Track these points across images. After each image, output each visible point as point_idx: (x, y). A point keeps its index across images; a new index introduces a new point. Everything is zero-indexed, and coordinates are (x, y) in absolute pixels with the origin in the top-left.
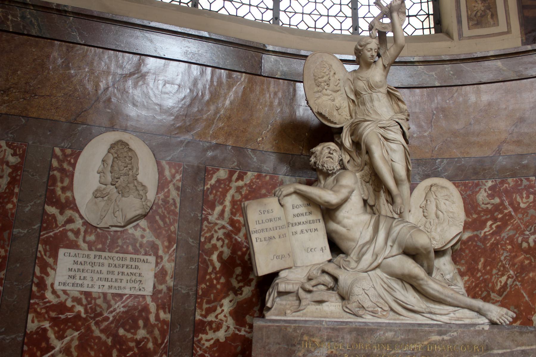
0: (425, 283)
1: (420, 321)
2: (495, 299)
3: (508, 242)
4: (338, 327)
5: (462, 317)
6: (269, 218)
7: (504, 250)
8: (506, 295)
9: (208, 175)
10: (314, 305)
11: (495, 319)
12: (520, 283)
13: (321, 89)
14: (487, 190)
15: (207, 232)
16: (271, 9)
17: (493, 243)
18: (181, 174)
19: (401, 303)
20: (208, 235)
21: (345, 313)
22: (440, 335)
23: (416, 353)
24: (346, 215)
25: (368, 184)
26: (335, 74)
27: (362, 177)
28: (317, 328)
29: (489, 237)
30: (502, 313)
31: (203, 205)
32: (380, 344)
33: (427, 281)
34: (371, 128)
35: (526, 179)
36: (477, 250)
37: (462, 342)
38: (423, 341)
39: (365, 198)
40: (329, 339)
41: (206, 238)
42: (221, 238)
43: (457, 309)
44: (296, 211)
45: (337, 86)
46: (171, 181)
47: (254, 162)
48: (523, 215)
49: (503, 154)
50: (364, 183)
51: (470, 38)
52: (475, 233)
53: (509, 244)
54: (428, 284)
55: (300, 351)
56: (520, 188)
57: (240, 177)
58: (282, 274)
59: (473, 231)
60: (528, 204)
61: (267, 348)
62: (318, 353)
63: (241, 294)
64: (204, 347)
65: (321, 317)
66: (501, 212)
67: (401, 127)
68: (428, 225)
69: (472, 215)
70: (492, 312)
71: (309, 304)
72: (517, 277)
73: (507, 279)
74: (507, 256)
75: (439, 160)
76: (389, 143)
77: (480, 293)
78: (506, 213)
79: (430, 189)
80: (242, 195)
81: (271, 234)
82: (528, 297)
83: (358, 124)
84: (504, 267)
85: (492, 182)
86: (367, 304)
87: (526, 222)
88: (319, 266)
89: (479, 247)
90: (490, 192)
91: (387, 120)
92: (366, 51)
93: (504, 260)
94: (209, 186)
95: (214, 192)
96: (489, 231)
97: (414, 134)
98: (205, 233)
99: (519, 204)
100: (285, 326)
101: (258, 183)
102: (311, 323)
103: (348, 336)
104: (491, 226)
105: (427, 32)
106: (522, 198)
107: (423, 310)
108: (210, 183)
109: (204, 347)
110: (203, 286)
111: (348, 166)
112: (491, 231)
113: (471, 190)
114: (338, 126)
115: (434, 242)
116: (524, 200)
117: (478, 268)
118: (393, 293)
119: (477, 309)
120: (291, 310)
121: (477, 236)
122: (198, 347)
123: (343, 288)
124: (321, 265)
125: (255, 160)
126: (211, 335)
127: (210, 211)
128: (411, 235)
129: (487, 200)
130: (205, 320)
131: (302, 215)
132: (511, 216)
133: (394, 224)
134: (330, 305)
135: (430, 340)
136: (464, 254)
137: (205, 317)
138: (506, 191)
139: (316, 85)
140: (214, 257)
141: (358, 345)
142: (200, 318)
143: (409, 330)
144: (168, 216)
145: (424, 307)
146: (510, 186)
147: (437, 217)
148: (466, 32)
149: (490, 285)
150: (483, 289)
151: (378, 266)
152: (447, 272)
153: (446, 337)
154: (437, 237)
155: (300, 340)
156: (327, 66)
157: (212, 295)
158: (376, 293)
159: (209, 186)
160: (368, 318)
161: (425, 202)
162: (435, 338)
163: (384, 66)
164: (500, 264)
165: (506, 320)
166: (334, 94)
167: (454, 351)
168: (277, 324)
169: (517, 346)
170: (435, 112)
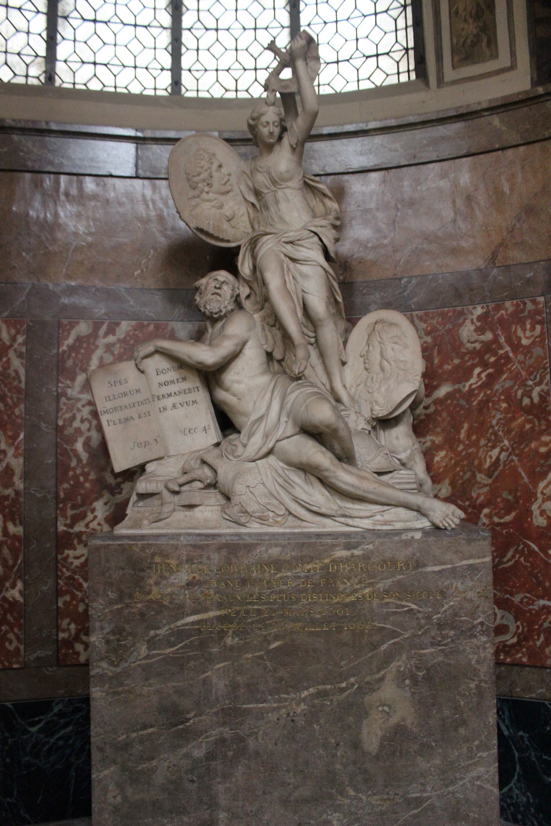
0: (332, 475)
1: (330, 527)
3: (502, 397)
5: (394, 519)
7: (497, 410)
8: (498, 476)
10: (183, 511)
11: (438, 522)
12: (517, 458)
14: (475, 321)
15: (67, 412)
16: (168, 70)
18: (24, 334)
20: (67, 416)
21: (225, 521)
23: (312, 576)
24: (236, 377)
25: (274, 328)
26: (220, 166)
27: (264, 319)
28: (172, 545)
29: (476, 392)
30: (448, 512)
31: (58, 375)
32: (260, 564)
33: (334, 472)
34: (269, 246)
35: (531, 301)
36: (458, 412)
37: (381, 557)
38: (324, 559)
39: (269, 350)
40: (190, 560)
41: (65, 420)
42: (87, 419)
43: (386, 508)
44: (163, 378)
45: (225, 184)
46: (11, 346)
47: (132, 307)
48: (526, 355)
49: (500, 265)
50: (266, 328)
51: (455, 82)
52: (457, 386)
53: (505, 401)
54: (336, 477)
55: (151, 577)
56: (522, 315)
57: (111, 331)
58: (150, 468)
59: (454, 384)
60: (532, 339)
61: (107, 574)
62: (175, 579)
63: (120, 493)
64: (73, 567)
65: (190, 528)
66: (495, 354)
67: (321, 240)
68: (369, 383)
69: (452, 360)
70: (434, 512)
71: (174, 510)
72: (513, 449)
73: (500, 453)
74: (500, 419)
75: (405, 280)
76: (298, 265)
77: (461, 474)
78: (501, 355)
79: (374, 329)
81: (127, 413)
82: (529, 478)
83: (258, 239)
84: (495, 434)
85: (483, 308)
86: (252, 507)
87: (529, 367)
88: (197, 454)
90: (478, 324)
91: (296, 231)
92: (260, 127)
93: (497, 424)
95: (74, 355)
97: (368, 242)
98: (63, 414)
99: (520, 339)
100: (128, 544)
102: (165, 539)
104: (479, 375)
105: (404, 78)
106: (524, 330)
107: (334, 513)
108: (66, 343)
109: (73, 567)
110: (66, 486)
111: (247, 304)
114: (233, 245)
115: (377, 408)
116: (528, 333)
117: (459, 438)
118: (291, 490)
119: (416, 508)
120: (149, 520)
121: (459, 391)
123: (224, 486)
124: (201, 452)
125: (132, 303)
126: (81, 550)
127: (68, 382)
128: (306, 406)
129: (475, 337)
130: (71, 531)
131: (172, 382)
132: (508, 360)
133: (288, 392)
134: (204, 510)
136: (440, 419)
137: (71, 526)
138: (501, 321)
139: (191, 186)
140: (79, 446)
141: (230, 566)
142: (65, 529)
143: (303, 544)
144: (9, 394)
145: (335, 507)
146: (509, 312)
147: (383, 369)
148: (449, 74)
149: (476, 462)
150: (466, 468)
151: (270, 452)
152: (401, 449)
153: (357, 552)
154: (381, 400)
155: (150, 563)
156: (206, 156)
157: (79, 498)
158: (266, 490)
159: (65, 348)
160: (255, 527)
161: (367, 348)
163: (292, 146)
164: (491, 431)
165: (451, 522)
166: (222, 198)
167: (368, 571)
168: (119, 543)
170: (400, 206)
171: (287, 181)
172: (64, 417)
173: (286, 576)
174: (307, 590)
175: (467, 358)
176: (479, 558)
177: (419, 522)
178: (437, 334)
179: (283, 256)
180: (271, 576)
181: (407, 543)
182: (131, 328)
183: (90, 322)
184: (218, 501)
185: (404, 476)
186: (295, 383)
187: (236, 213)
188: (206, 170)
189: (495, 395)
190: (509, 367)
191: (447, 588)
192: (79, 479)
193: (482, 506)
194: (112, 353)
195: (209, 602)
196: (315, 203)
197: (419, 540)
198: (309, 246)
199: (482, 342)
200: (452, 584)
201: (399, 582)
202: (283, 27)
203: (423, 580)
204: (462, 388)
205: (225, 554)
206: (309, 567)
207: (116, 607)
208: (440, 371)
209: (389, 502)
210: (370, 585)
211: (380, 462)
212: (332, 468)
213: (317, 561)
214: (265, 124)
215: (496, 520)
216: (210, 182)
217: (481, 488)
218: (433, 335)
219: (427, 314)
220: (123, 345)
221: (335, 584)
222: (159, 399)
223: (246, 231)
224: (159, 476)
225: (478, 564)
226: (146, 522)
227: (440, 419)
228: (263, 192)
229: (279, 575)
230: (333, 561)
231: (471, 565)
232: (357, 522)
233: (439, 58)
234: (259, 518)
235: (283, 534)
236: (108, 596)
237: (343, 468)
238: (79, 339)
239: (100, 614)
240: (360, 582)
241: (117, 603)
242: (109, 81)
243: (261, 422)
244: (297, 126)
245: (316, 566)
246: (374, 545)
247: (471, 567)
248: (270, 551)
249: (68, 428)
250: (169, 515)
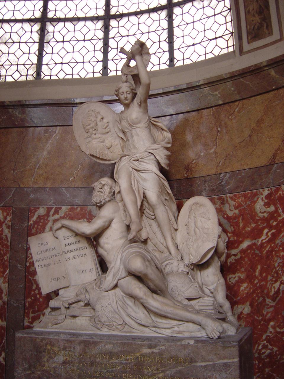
0: (145, 301)
2: (270, 304)
3: (281, 248)
4: (71, 339)
5: (185, 330)
6: (45, 249)
7: (278, 256)
8: (279, 301)
9: (31, 214)
13: (90, 135)
14: (264, 199)
16: (101, 61)
17: (268, 251)
18: (11, 216)
19: (133, 318)
21: (91, 326)
22: (151, 348)
26: (102, 119)
28: (56, 339)
29: (265, 245)
32: (101, 354)
33: (146, 300)
34: (124, 163)
36: (254, 258)
37: (169, 355)
39: (127, 224)
40: (65, 349)
43: (181, 323)
44: (67, 241)
45: (106, 128)
46: (4, 222)
51: (249, 51)
52: (254, 241)
58: (61, 292)
61: (24, 354)
65: (72, 329)
66: (276, 220)
69: (251, 225)
70: (207, 327)
73: (280, 285)
74: (280, 263)
75: (223, 175)
76: (140, 173)
77: (257, 298)
84: (277, 272)
85: (268, 190)
89: (257, 255)
90: (266, 201)
93: (278, 266)
94: (31, 222)
95: (36, 226)
96: (265, 239)
101: (71, 215)
102: (52, 335)
103: (78, 347)
108: (32, 219)
110: (29, 300)
112: (267, 239)
113: (250, 201)
115: (192, 257)
117: (255, 275)
120: (52, 324)
121: (254, 244)
124: (86, 284)
125: (68, 196)
129: (264, 209)
131: (73, 243)
135: (141, 352)
136: (244, 262)
139: (86, 132)
142: (28, 324)
143: (125, 343)
144: (2, 249)
147: (195, 233)
149: (266, 291)
151: (116, 286)
153: (155, 350)
154: (194, 253)
155: (45, 349)
157: (36, 307)
159: (31, 222)
160: (105, 331)
162: (146, 351)
164: (274, 270)
166: (104, 136)
168: (31, 336)
169: (220, 359)
170: (219, 129)
171: (137, 124)
172: (30, 261)
173: (115, 362)
174: (126, 371)
175: (260, 223)
176: (230, 359)
177: (199, 333)
178: (241, 208)
179: (131, 169)
180: (107, 361)
181: (185, 347)
182: (67, 210)
183: (45, 207)
184: (91, 314)
185: (206, 301)
187: (113, 144)
188: (93, 122)
189: (276, 247)
192: (37, 296)
193: (270, 320)
195: (74, 375)
196: (158, 134)
197: (191, 345)
198: (147, 162)
199: (269, 212)
200: (213, 375)
201: (180, 371)
202: (164, 29)
203: (194, 371)
204: (256, 242)
205: (83, 346)
206: (128, 358)
207: (27, 373)
208: (244, 232)
209: (182, 319)
210: (163, 371)
211: (191, 292)
212: (145, 297)
213: (132, 354)
214: (122, 93)
215: (278, 330)
216: (96, 128)
217: (268, 308)
218: (239, 208)
219: (235, 196)
221: (143, 369)
222: (65, 253)
223: (119, 153)
224: (64, 298)
225: (230, 362)
226: (50, 324)
227: (244, 262)
228: (126, 131)
229: (111, 361)
230: (141, 355)
231: (224, 363)
232: (162, 331)
234: (107, 325)
235: (121, 336)
236: (24, 366)
237: (153, 297)
238: (39, 217)
239: (20, 376)
240: (157, 369)
241: (28, 370)
244: (140, 91)
245: (131, 357)
246: (165, 347)
247: (225, 364)
248: (107, 346)
249: (32, 267)
250: (62, 321)
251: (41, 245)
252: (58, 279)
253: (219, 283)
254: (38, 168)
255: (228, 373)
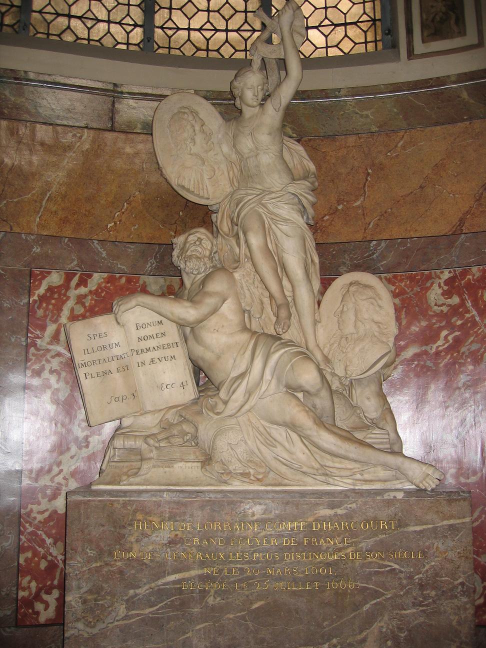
9: (34, 282)
14: (442, 285)
15: (35, 363)
23: (296, 534)
28: (155, 502)
32: (244, 523)
34: (251, 206)
37: (364, 517)
38: (308, 518)
40: (172, 517)
47: (104, 258)
49: (467, 231)
52: (424, 348)
57: (83, 282)
59: (422, 346)
61: (86, 531)
64: (36, 522)
66: (461, 316)
75: (374, 243)
79: (348, 291)
80: (85, 307)
85: (450, 272)
90: (446, 288)
94: (36, 298)
96: (444, 345)
98: (32, 365)
101: (109, 289)
102: (147, 495)
103: (200, 513)
104: (446, 337)
108: (37, 292)
112: (446, 345)
113: (419, 286)
121: (426, 353)
122: (27, 522)
125: (104, 254)
127: (38, 332)
128: (292, 365)
129: (442, 300)
131: (152, 337)
132: (475, 324)
133: (272, 350)
137: (36, 480)
138: (469, 285)
142: (29, 482)
153: (340, 511)
155: (131, 520)
159: (36, 298)
160: (237, 485)
169: (443, 519)
170: (370, 171)
176: (459, 518)
181: (389, 503)
182: (103, 280)
183: (62, 273)
186: (278, 342)
190: (475, 330)
191: (429, 548)
194: (83, 304)
199: (449, 305)
201: (381, 541)
218: (401, 297)
219: (395, 277)
220: (94, 297)
221: (318, 543)
225: (458, 524)
230: (316, 520)
231: (451, 526)
233: (410, 31)
236: (86, 553)
239: (78, 572)
241: (96, 561)
242: (82, 31)
243: (243, 379)
246: (357, 504)
251: (93, 338)
252: (124, 398)
253: (385, 408)
254: (48, 200)
255: (455, 540)
